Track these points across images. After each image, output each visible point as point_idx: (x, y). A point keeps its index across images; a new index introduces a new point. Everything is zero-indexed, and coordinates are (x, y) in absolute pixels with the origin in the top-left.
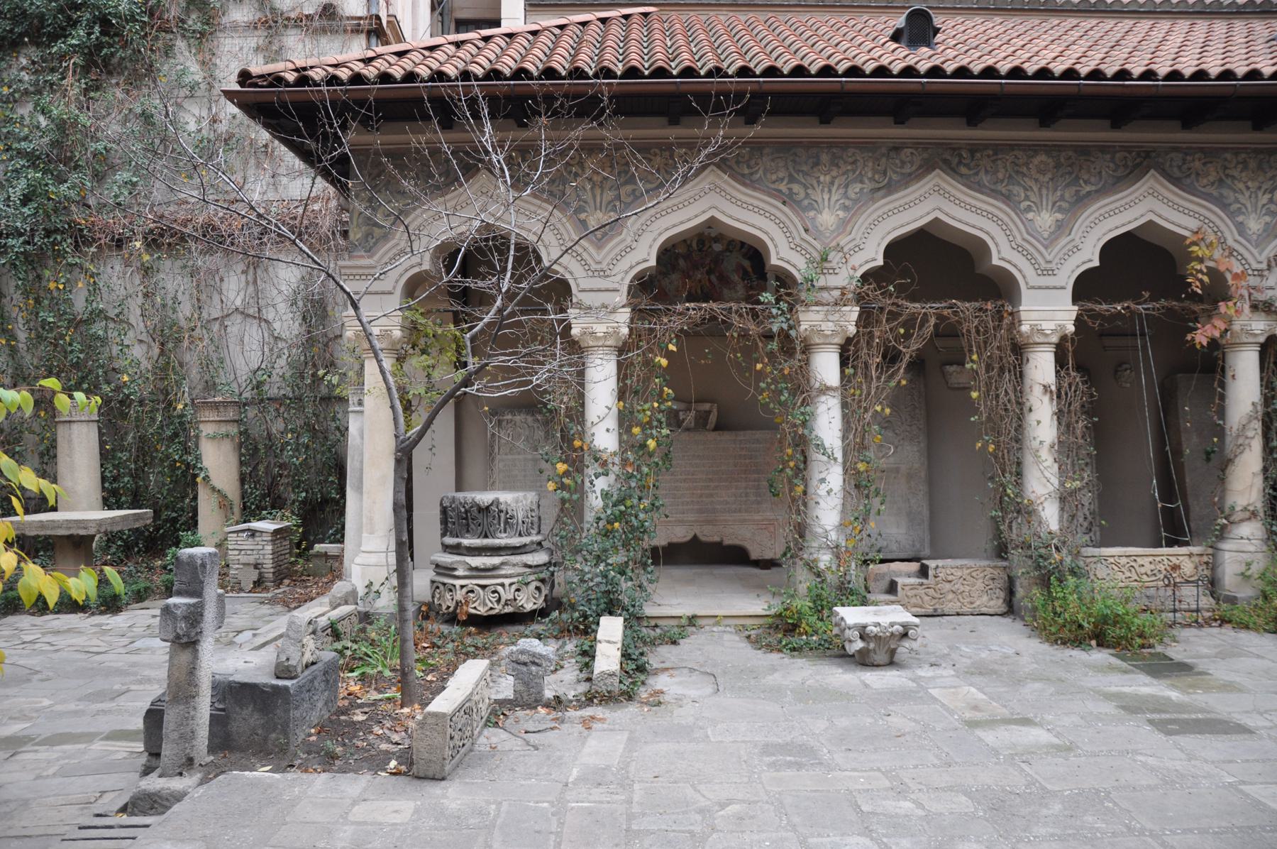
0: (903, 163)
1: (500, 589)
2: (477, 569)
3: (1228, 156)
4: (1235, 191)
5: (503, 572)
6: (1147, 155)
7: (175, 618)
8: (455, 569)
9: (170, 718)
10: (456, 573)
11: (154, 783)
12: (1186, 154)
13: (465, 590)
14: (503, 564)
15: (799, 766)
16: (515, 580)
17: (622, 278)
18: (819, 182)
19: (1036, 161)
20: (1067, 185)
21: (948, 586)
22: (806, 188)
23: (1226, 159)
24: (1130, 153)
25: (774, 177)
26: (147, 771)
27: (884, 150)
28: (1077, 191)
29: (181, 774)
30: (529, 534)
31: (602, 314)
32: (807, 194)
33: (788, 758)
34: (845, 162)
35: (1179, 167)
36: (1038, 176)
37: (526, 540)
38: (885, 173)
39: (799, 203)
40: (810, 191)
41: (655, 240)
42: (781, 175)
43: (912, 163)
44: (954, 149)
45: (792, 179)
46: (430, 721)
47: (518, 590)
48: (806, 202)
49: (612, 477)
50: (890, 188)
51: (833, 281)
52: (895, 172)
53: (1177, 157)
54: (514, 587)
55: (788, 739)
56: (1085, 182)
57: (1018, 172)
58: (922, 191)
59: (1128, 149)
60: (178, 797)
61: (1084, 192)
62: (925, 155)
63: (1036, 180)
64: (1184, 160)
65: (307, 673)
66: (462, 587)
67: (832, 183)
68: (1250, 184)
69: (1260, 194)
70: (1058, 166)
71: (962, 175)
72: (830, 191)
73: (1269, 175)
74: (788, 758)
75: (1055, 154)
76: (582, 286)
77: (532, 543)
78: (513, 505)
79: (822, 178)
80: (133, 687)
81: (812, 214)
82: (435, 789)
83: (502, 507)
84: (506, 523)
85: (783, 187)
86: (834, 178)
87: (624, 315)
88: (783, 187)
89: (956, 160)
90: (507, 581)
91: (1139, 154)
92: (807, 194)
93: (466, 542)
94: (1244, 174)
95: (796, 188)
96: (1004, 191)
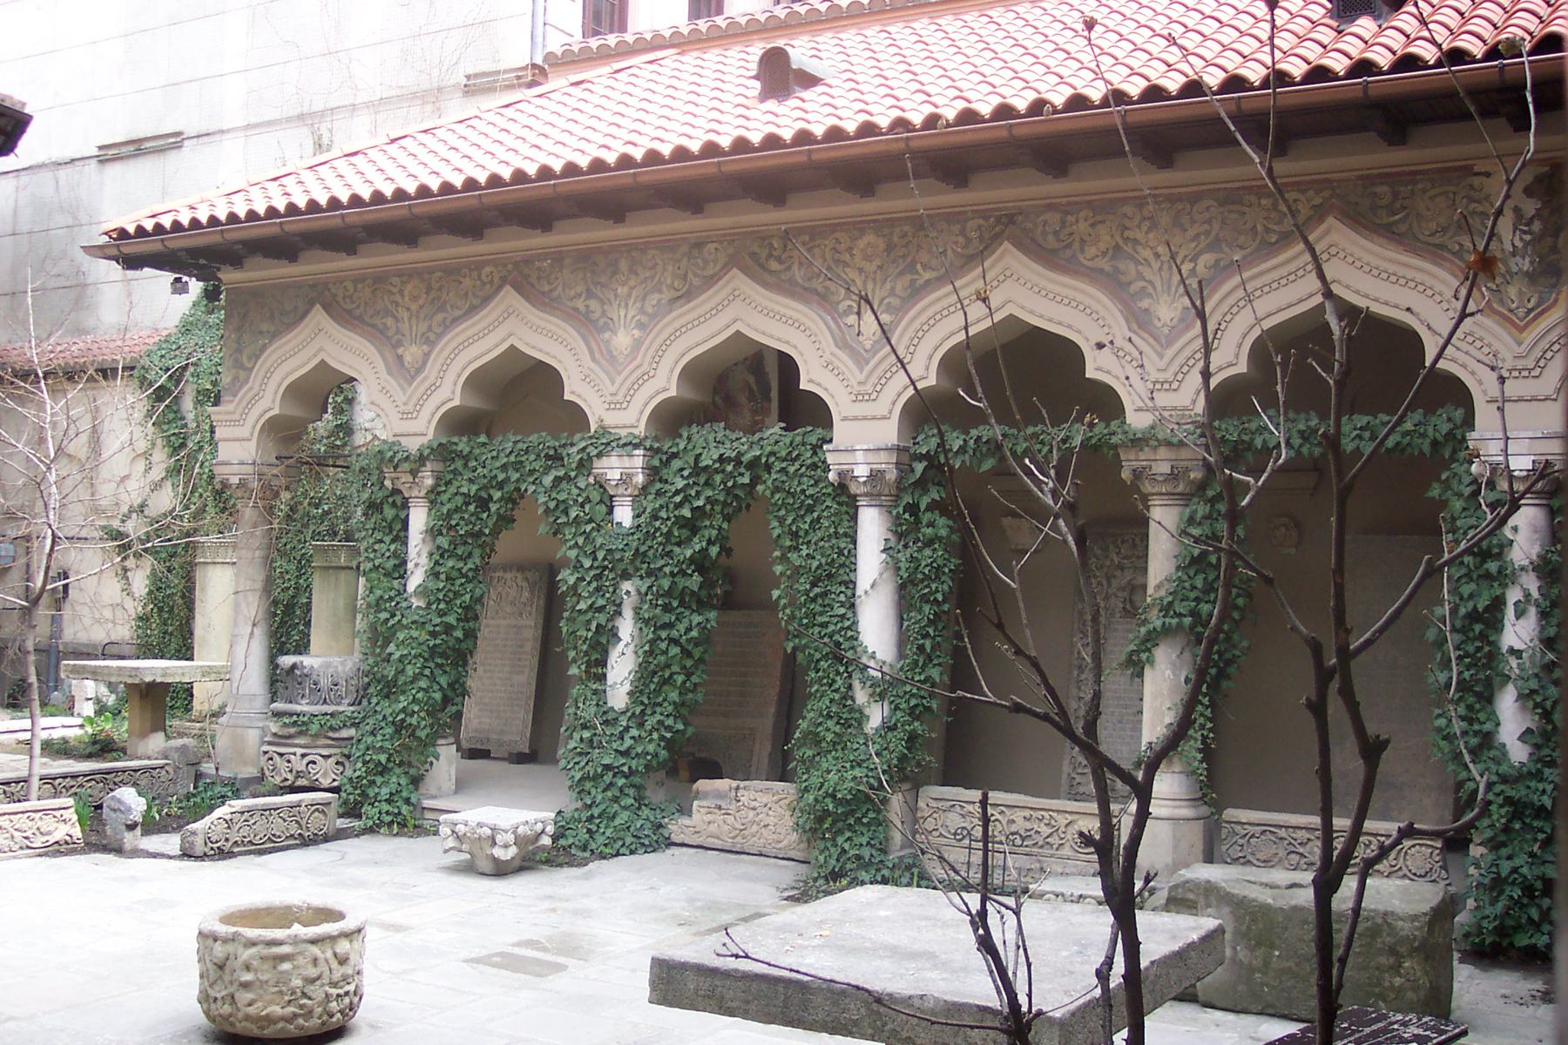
0: (706, 262)
3: (1128, 210)
4: (1138, 262)
6: (1011, 219)
12: (1067, 213)
18: (616, 296)
19: (861, 243)
20: (901, 273)
21: (751, 814)
22: (603, 303)
23: (1125, 215)
24: (986, 218)
27: (685, 248)
28: (913, 281)
32: (604, 312)
35: (1056, 233)
36: (864, 264)
38: (685, 277)
39: (594, 322)
42: (579, 289)
43: (715, 261)
44: (764, 239)
45: (590, 295)
50: (688, 296)
52: (696, 275)
53: (1054, 218)
56: (925, 267)
57: (837, 262)
58: (717, 299)
59: (984, 215)
61: (921, 282)
62: (731, 250)
63: (861, 270)
64: (1063, 223)
67: (629, 295)
70: (890, 248)
71: (771, 272)
73: (1191, 233)
75: (886, 231)
81: (607, 335)
85: (580, 304)
86: (632, 288)
88: (580, 304)
89: (764, 254)
91: (998, 220)
94: (1151, 236)
95: (593, 304)
96: (820, 289)
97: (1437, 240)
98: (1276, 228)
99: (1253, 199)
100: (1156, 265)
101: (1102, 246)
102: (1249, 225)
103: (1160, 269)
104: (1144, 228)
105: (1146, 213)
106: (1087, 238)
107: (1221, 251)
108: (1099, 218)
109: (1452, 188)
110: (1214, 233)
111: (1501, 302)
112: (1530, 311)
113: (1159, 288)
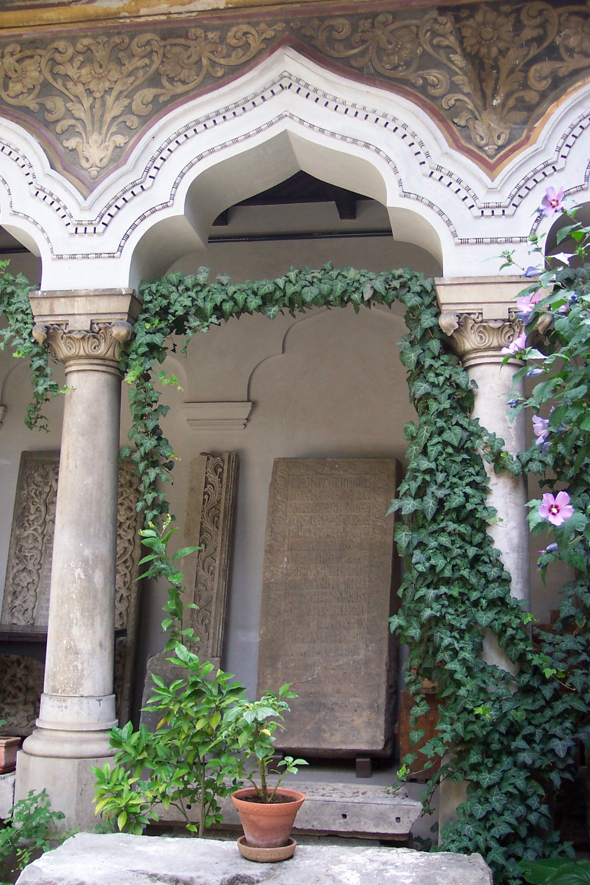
3: (61, 45)
68: (92, 86)
69: (110, 99)
94: (84, 71)
97: (401, 73)
98: (222, 61)
99: (199, 32)
100: (87, 102)
101: (29, 83)
102: (194, 58)
103: (92, 107)
104: (76, 63)
105: (79, 47)
106: (14, 75)
107: (163, 87)
108: (28, 53)
109: (414, 22)
110: (155, 66)
111: (469, 139)
112: (500, 148)
113: (89, 128)
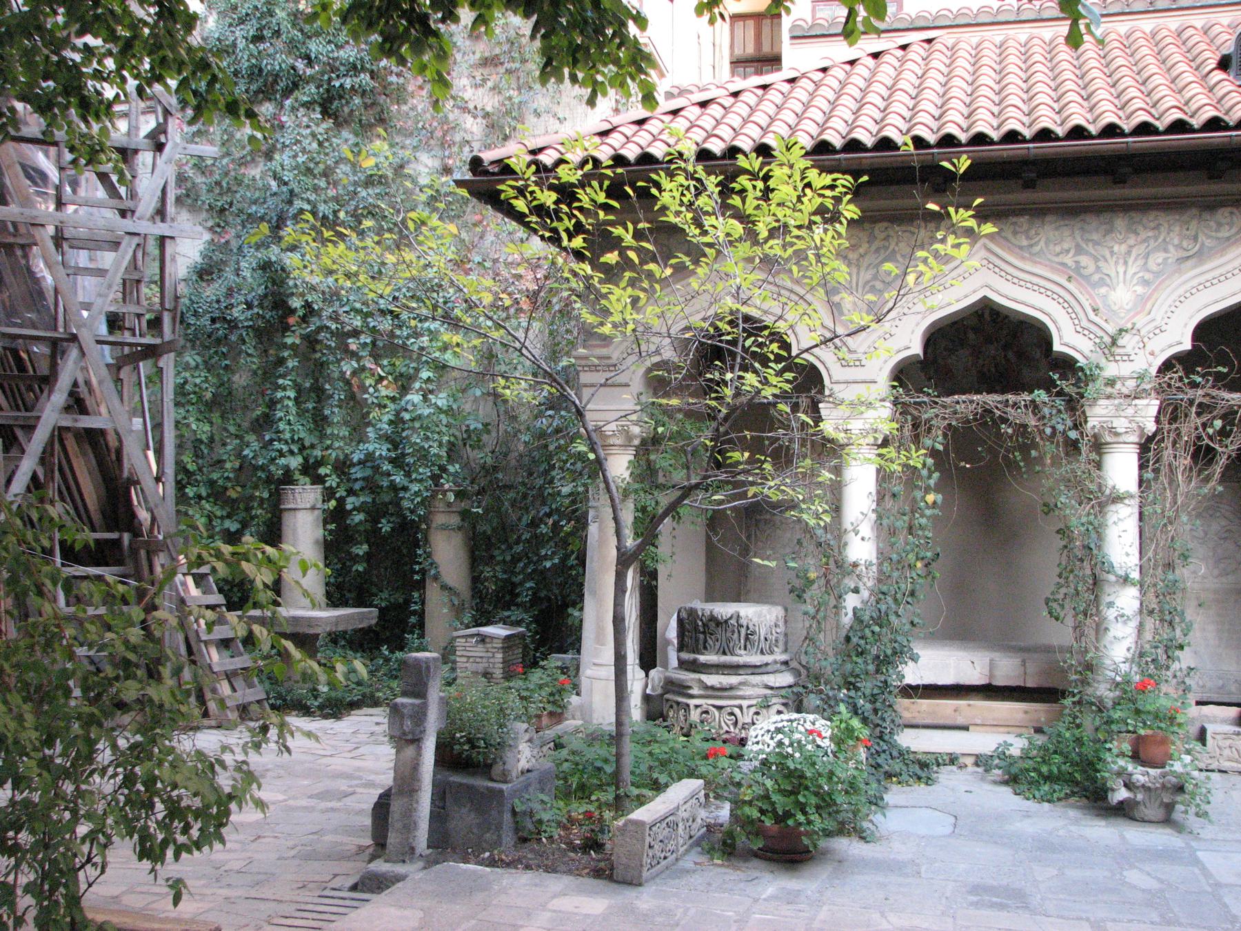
1: (737, 711)
2: (712, 688)
5: (740, 693)
7: (402, 717)
8: (690, 687)
9: (396, 806)
10: (691, 692)
11: (380, 866)
13: (699, 710)
14: (740, 684)
15: (1002, 907)
16: (754, 702)
17: (880, 369)
18: (1112, 253)
22: (1096, 260)
25: (1058, 249)
26: (373, 858)
29: (404, 861)
30: (772, 653)
31: (860, 405)
32: (1098, 268)
33: (994, 899)
34: (1145, 228)
37: (768, 658)
39: (1087, 278)
40: (1101, 264)
41: (918, 324)
42: (1066, 246)
45: (1079, 250)
46: (630, 827)
47: (757, 713)
48: (1096, 277)
49: (865, 594)
51: (1125, 369)
54: (753, 710)
55: (1005, 882)
60: (399, 878)
65: (521, 779)
66: (697, 706)
67: (1129, 253)
72: (1126, 263)
74: (994, 899)
76: (835, 378)
77: (775, 662)
78: (755, 620)
79: (1116, 248)
80: (359, 790)
81: (1103, 290)
82: (630, 894)
83: (744, 622)
84: (747, 639)
85: (1069, 260)
86: (1131, 247)
87: (886, 410)
90: (745, 703)
92: (1098, 268)
93: (702, 658)
95: (1084, 260)
